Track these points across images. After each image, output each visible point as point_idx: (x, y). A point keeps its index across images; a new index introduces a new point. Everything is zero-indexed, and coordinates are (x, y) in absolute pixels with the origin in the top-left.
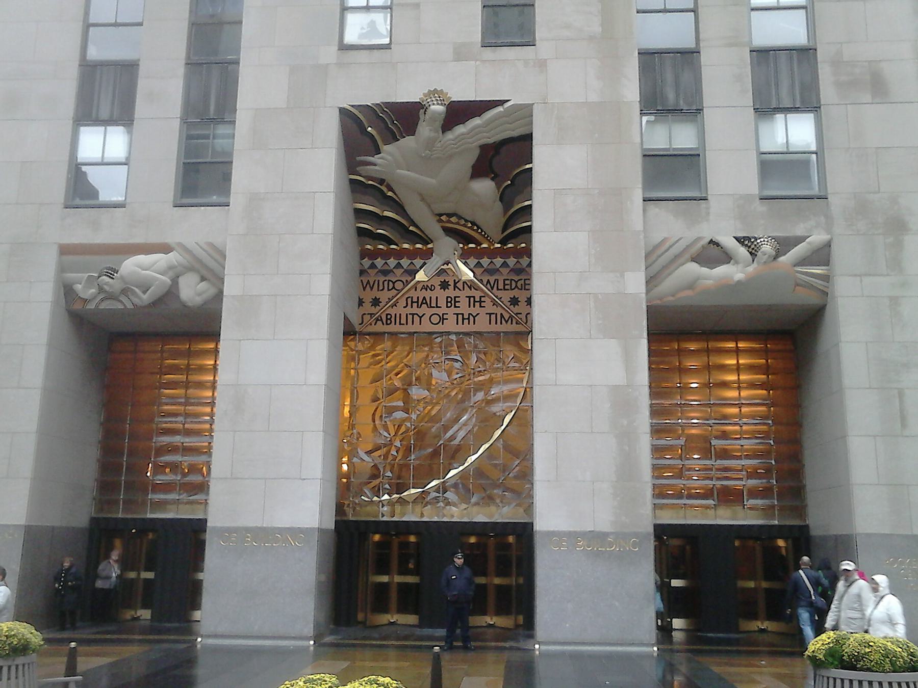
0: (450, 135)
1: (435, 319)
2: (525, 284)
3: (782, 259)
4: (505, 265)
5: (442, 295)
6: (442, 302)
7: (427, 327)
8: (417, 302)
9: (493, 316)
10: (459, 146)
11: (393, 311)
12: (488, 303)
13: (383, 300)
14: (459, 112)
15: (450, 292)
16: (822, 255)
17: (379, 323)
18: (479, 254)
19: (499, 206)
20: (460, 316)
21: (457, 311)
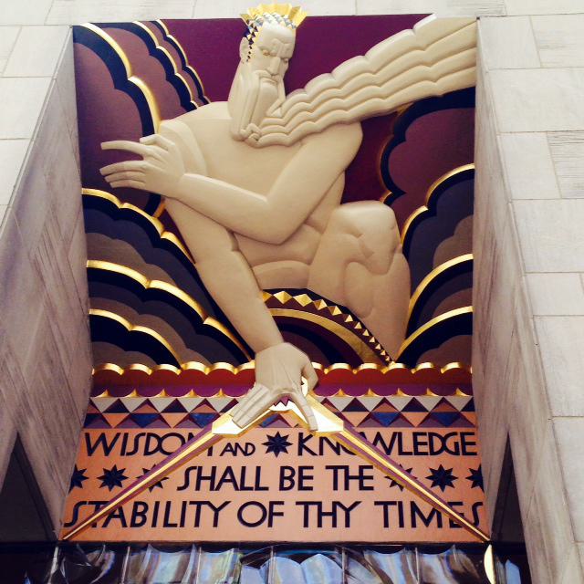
0: (297, 95)
1: (253, 514)
2: (464, 444)
4: (414, 406)
5: (271, 465)
6: (270, 478)
7: (230, 530)
8: (212, 478)
9: (393, 510)
11: (149, 498)
15: (291, 458)
17: (116, 522)
20: (313, 510)
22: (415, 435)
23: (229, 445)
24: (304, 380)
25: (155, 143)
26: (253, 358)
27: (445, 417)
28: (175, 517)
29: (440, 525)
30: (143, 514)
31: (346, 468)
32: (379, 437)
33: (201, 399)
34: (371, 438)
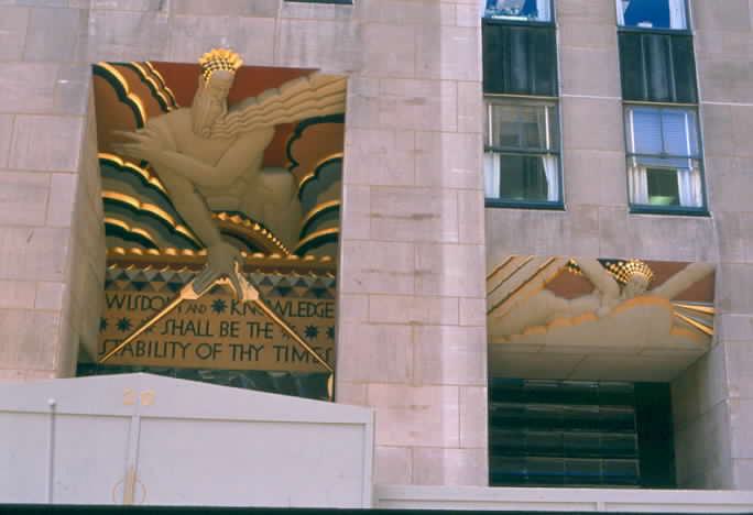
0: (235, 113)
1: (204, 351)
3: (658, 290)
4: (301, 283)
5: (215, 320)
9: (283, 351)
10: (249, 125)
12: (276, 333)
13: (135, 323)
14: (251, 82)
16: (704, 289)
17: (127, 352)
18: (268, 269)
19: (295, 202)
20: (239, 349)
21: (235, 341)
22: (300, 303)
23: (191, 305)
24: (237, 264)
25: (144, 134)
26: (205, 246)
27: (319, 292)
28: (161, 352)
29: (307, 360)
30: (143, 349)
31: (258, 324)
32: (278, 303)
33: (173, 272)
34: (274, 304)
